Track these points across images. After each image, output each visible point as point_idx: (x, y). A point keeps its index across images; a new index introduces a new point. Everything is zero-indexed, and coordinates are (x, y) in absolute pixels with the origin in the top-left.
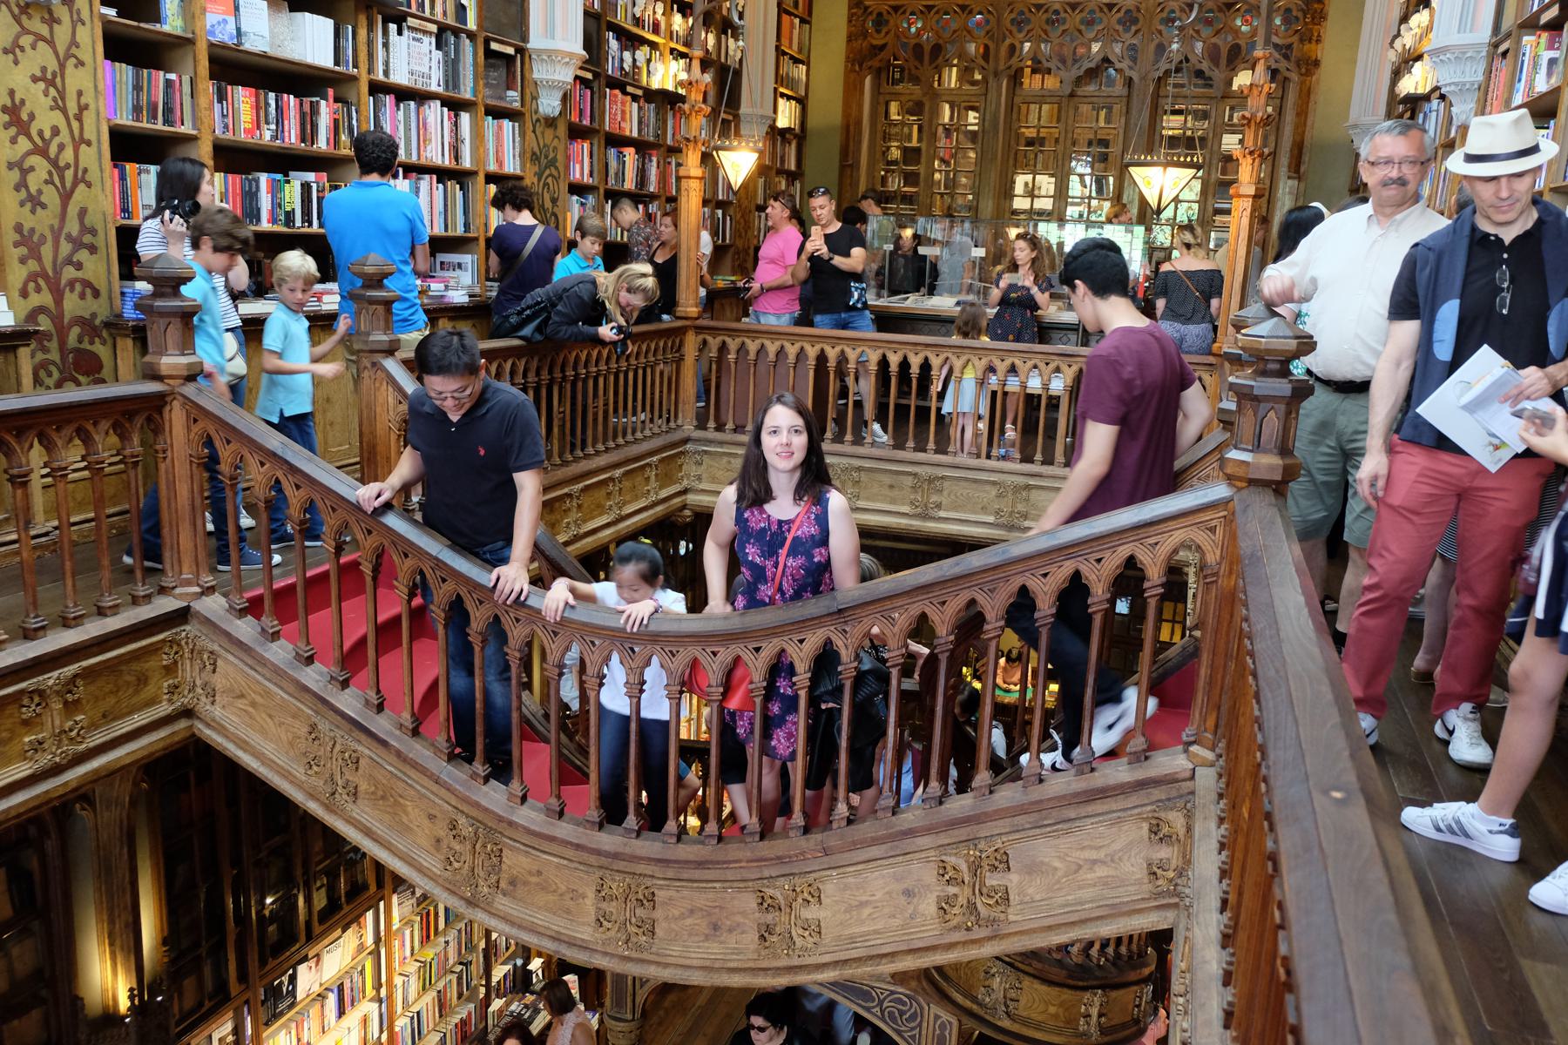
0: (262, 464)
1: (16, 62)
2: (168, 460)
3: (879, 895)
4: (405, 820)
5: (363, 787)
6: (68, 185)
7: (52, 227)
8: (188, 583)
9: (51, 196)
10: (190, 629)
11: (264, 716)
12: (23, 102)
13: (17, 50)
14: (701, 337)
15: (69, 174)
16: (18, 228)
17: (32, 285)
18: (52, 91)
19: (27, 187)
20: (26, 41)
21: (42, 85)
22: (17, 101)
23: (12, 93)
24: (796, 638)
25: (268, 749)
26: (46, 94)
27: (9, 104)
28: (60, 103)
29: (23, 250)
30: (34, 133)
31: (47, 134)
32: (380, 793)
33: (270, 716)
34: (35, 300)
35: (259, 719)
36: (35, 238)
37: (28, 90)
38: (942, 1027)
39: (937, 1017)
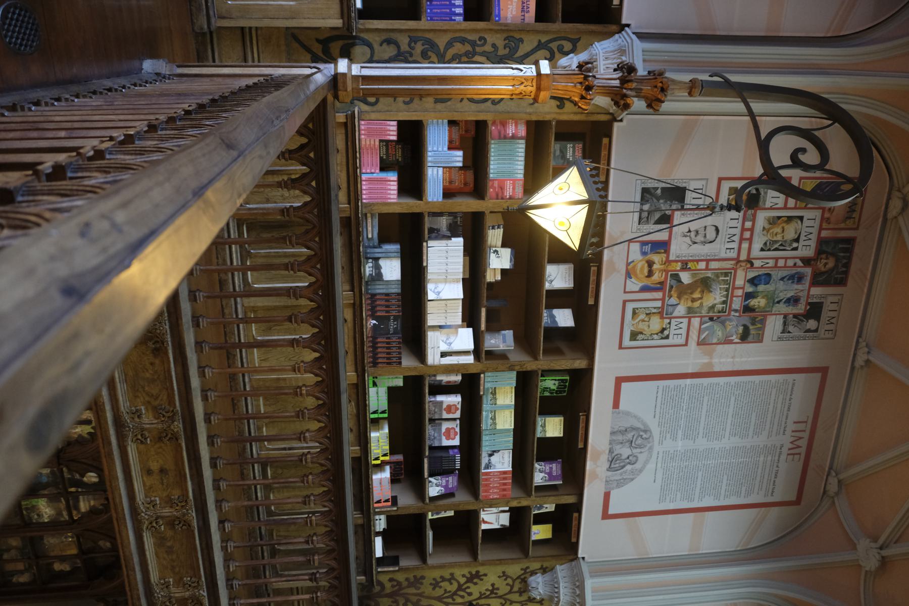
1: (499, 577)
6: (445, 600)
7: (424, 592)
9: (439, 592)
12: (482, 580)
13: (505, 578)
15: (450, 600)
16: (423, 577)
17: (395, 583)
18: (488, 593)
19: (442, 581)
20: (510, 581)
21: (490, 588)
22: (482, 577)
23: (485, 575)
26: (487, 590)
27: (480, 574)
28: (483, 596)
29: (412, 580)
30: (468, 585)
31: (468, 590)
34: (388, 585)
36: (418, 585)
37: (488, 582)
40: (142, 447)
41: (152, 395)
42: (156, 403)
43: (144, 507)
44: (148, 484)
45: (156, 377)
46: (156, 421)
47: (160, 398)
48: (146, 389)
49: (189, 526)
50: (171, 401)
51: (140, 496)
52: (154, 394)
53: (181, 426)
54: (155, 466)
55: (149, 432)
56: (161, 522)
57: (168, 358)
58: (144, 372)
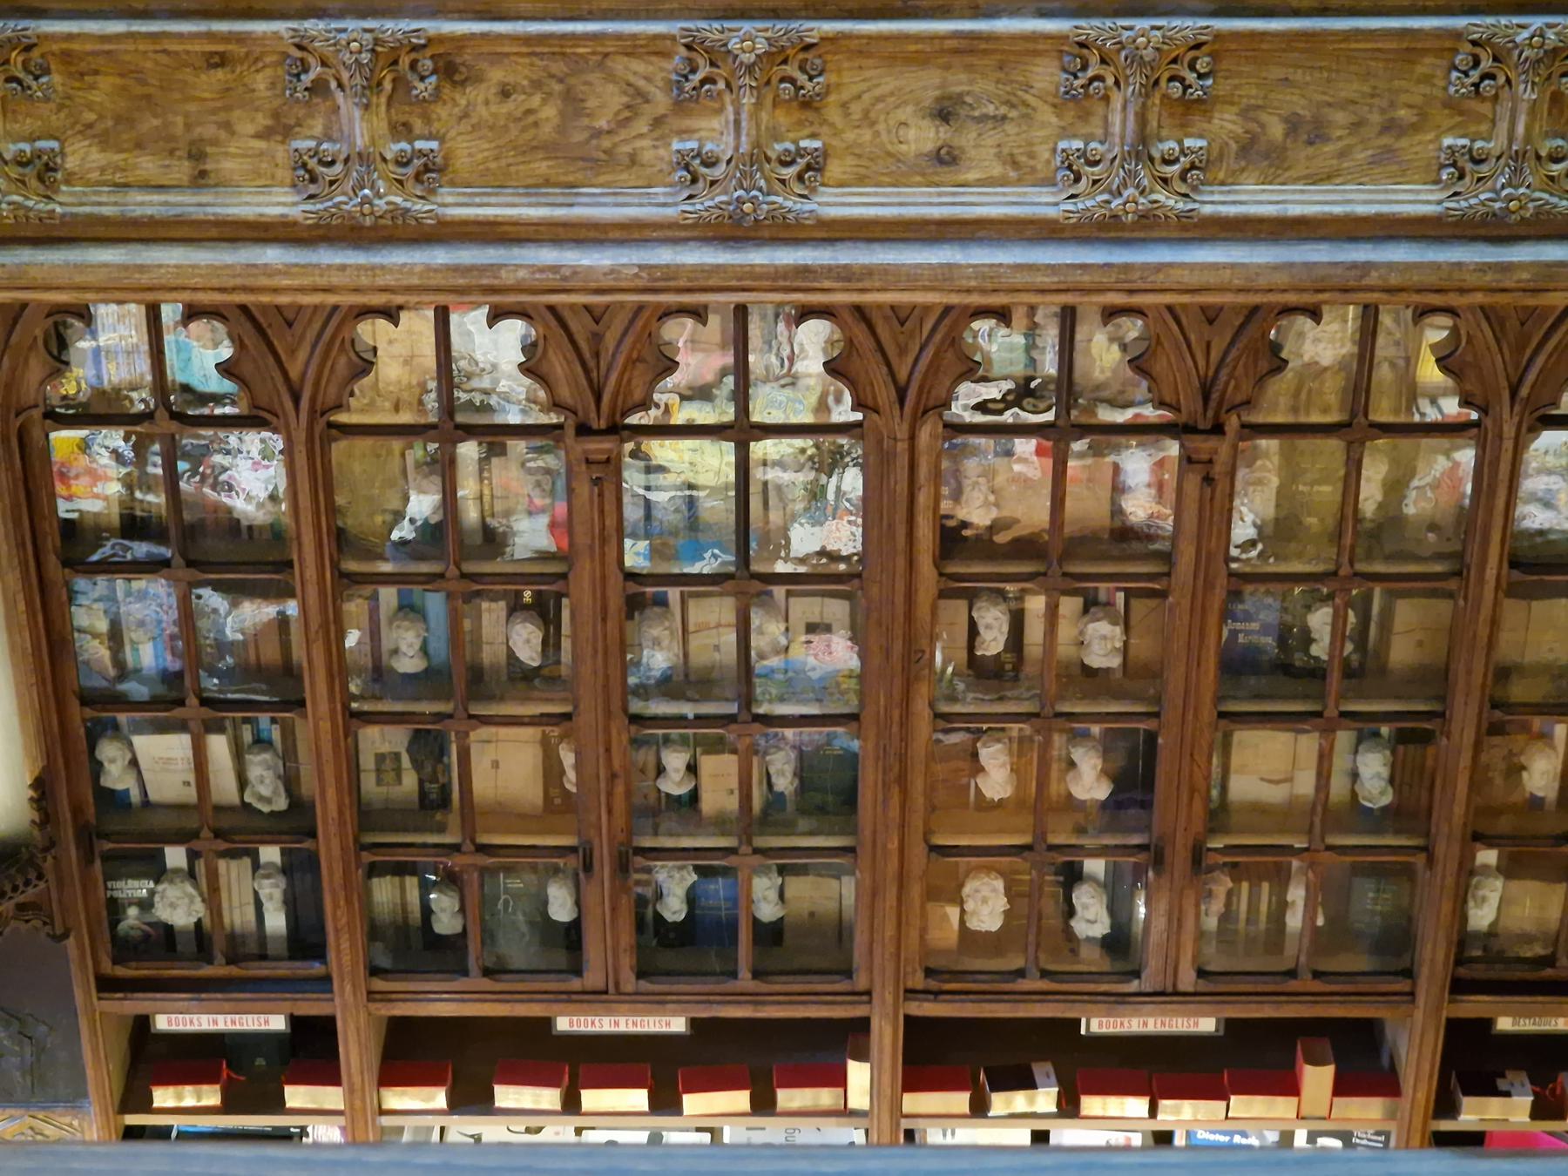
40: (834, 169)
41: (628, 107)
42: (661, 101)
43: (1090, 195)
44: (997, 170)
45: (557, 87)
46: (730, 109)
47: (641, 83)
48: (602, 123)
49: (1198, 46)
50: (655, 48)
51: (1045, 203)
52: (625, 99)
53: (747, 26)
54: (923, 136)
55: (777, 138)
56: (1172, 144)
57: (473, 36)
58: (536, 124)
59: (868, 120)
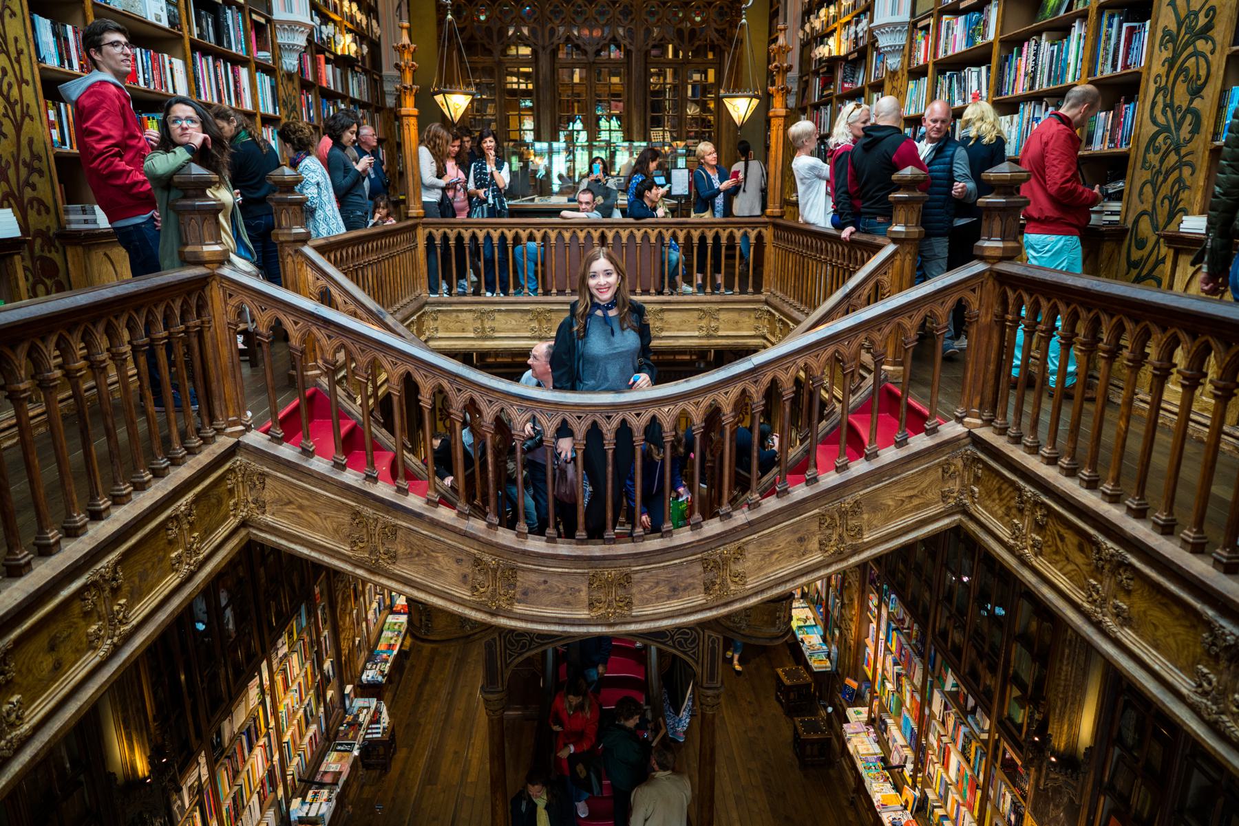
0: (296, 323)
2: (212, 329)
3: (783, 545)
4: (437, 567)
5: (401, 550)
7: (13, 156)
8: (235, 424)
10: (240, 459)
11: (311, 514)
14: (427, 231)
15: (18, 108)
24: (723, 391)
25: (318, 538)
32: (415, 552)
33: (317, 514)
35: (306, 517)
38: (713, 642)
39: (709, 637)
51: (91, 659)
59: (29, 671)
